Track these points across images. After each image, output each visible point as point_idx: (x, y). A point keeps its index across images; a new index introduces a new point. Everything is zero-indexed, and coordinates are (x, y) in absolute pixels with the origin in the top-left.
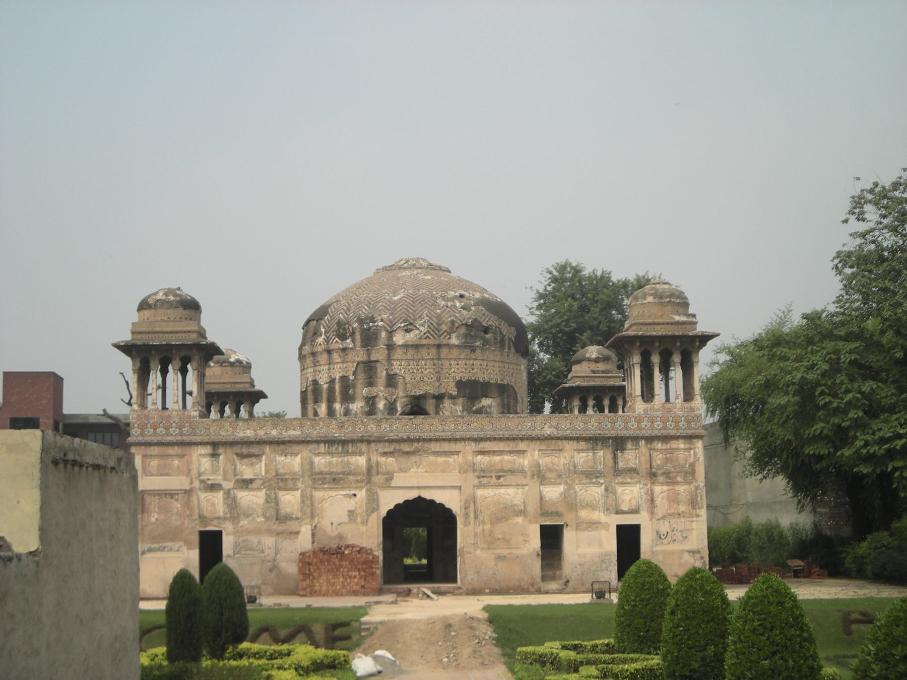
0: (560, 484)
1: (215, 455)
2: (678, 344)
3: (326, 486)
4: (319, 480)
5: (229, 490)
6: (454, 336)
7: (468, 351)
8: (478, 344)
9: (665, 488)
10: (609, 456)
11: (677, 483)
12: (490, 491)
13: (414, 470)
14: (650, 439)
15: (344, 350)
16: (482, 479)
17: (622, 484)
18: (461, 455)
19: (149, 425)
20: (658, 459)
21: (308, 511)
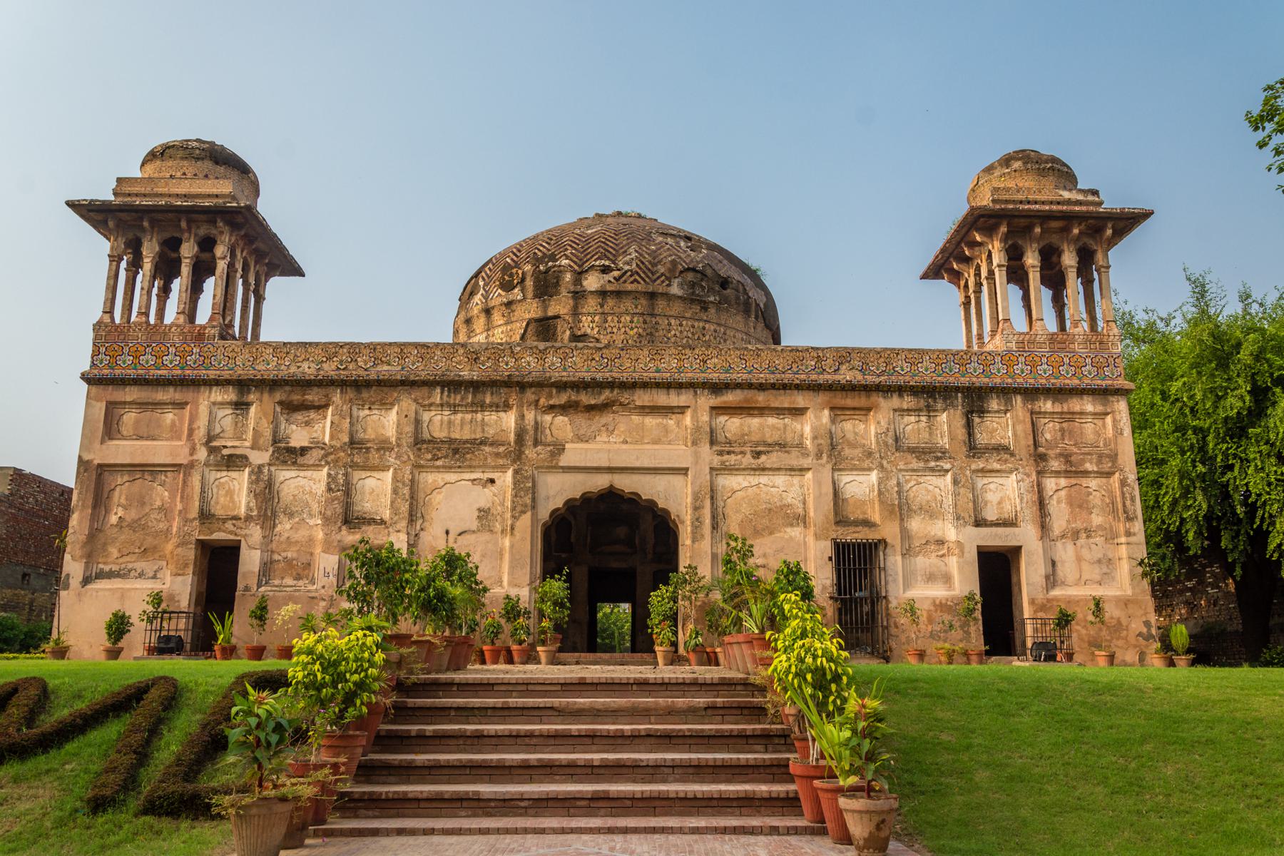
0: (870, 469)
1: (241, 406)
2: (1076, 231)
3: (439, 463)
4: (428, 451)
5: (260, 467)
6: (676, 282)
7: (697, 308)
8: (712, 299)
9: (1063, 482)
10: (960, 422)
11: (1086, 473)
12: (740, 479)
13: (603, 437)
14: (1031, 393)
15: (509, 304)
16: (726, 457)
17: (983, 471)
18: (689, 413)
19: (126, 350)
20: (1049, 431)
21: (404, 508)
